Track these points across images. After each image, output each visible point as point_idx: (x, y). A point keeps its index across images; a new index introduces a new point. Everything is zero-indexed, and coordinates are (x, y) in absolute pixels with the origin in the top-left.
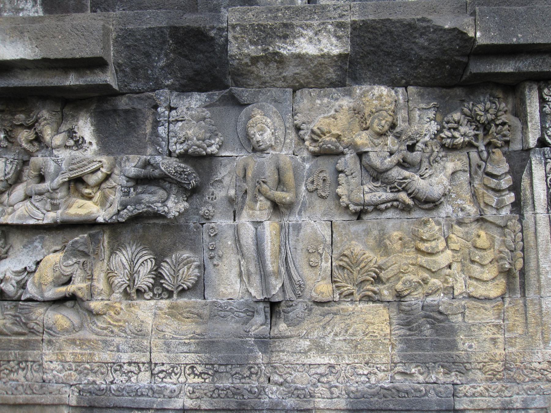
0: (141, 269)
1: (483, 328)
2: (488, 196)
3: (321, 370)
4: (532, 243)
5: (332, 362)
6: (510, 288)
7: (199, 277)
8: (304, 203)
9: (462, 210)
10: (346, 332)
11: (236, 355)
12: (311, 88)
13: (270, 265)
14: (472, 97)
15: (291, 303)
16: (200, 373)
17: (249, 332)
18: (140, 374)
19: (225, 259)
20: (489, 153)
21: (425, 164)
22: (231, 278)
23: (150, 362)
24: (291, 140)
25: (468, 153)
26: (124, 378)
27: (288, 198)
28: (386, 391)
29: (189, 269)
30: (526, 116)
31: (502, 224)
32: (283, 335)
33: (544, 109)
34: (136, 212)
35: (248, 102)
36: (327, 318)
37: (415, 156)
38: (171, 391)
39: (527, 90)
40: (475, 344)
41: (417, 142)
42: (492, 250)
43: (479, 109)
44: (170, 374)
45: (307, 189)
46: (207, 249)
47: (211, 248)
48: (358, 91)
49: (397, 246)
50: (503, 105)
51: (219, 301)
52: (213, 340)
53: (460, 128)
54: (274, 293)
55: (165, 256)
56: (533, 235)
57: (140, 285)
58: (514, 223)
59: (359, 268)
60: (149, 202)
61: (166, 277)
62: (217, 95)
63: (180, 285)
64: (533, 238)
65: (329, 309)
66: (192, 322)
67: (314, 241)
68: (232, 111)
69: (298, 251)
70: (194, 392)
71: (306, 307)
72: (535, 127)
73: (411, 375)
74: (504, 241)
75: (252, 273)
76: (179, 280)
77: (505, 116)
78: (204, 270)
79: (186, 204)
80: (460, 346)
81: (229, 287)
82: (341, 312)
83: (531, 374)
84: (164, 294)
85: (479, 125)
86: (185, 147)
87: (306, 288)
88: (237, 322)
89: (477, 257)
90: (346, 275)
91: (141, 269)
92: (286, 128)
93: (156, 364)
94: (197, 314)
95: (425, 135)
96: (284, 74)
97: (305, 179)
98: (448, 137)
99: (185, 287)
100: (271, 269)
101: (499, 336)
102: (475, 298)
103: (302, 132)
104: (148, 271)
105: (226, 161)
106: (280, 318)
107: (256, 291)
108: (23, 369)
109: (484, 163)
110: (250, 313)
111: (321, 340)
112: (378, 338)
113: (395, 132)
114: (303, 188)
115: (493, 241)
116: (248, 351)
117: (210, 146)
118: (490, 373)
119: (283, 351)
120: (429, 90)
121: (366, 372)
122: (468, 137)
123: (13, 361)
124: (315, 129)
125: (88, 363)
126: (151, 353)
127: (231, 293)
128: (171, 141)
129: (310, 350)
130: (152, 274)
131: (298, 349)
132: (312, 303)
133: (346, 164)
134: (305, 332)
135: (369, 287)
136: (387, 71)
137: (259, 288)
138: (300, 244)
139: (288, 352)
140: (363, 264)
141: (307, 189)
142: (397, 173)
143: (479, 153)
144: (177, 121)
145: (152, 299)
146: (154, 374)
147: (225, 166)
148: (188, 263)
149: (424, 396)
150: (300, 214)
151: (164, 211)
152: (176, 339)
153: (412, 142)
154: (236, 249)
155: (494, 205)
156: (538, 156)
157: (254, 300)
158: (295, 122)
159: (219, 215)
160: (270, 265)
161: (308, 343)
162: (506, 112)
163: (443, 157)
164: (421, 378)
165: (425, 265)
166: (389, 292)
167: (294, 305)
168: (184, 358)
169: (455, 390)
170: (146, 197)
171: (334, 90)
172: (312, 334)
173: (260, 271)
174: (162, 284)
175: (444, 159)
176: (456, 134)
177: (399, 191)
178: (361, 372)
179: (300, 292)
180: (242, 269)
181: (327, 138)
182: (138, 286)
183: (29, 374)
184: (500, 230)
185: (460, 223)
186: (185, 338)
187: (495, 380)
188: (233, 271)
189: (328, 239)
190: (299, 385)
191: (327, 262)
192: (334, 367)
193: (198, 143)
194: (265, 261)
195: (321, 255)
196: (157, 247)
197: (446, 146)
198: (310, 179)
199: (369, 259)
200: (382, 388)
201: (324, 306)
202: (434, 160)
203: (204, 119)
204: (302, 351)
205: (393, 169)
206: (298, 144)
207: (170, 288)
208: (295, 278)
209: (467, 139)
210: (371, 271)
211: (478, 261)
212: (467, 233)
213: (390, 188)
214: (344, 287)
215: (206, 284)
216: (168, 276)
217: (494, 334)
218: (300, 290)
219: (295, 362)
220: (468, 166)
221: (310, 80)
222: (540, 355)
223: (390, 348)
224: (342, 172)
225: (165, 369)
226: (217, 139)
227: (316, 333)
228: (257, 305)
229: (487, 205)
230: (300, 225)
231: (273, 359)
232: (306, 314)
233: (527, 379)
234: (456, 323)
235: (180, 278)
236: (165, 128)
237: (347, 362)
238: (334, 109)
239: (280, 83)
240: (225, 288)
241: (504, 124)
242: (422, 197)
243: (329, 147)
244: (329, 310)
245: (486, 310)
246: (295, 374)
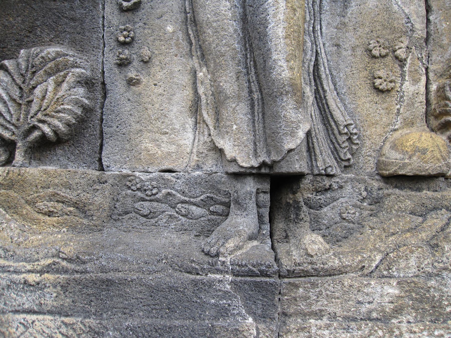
7: (87, 110)
11: (177, 323)
13: (282, 63)
15: (327, 182)
17: (217, 255)
19: (158, 68)
22: (172, 115)
29: (59, 84)
32: (319, 266)
46: (113, 44)
47: (122, 39)
51: (137, 174)
52: (111, 275)
54: (292, 146)
63: (34, 128)
65: (438, 195)
66: (61, 224)
67: (384, 27)
69: (344, 53)
71: (364, 194)
75: (227, 98)
76: (32, 111)
78: (105, 97)
81: (165, 138)
87: (363, 145)
88: (183, 230)
94: (75, 205)
99: (46, 129)
100: (286, 74)
106: (298, 220)
107: (238, 144)
110: (219, 208)
111: (432, 283)
116: (213, 313)
119: (319, 315)
127: (169, 154)
129: (398, 311)
131: (364, 309)
132: (382, 184)
134: (378, 258)
137: (247, 137)
138: (350, 35)
139: (333, 317)
154: (185, 44)
157: (233, 169)
160: (282, 63)
167: (335, 186)
168: (22, 329)
172: (403, 264)
179: (349, 156)
180: (201, 91)
186: (29, 267)
188: (177, 97)
191: (416, 81)
195: (402, 62)
201: (419, 190)
204: (374, 315)
215: (105, 129)
218: (350, 150)
227: (413, 262)
228: (239, 186)
232: (366, 213)
235: (34, 108)
240: (155, 140)
244: (436, 199)
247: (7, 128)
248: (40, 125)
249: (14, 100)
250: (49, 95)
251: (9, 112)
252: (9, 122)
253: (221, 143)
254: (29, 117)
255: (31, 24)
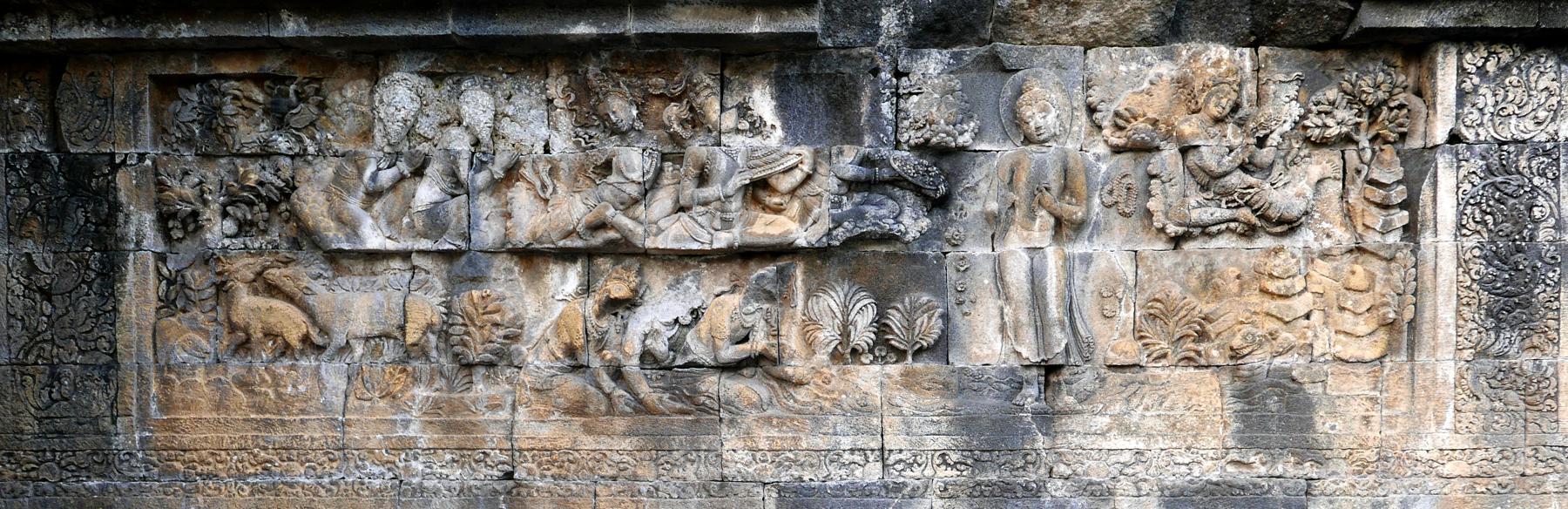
0: (859, 318)
1: (1352, 401)
2: (1371, 214)
3: (1126, 457)
4: (1429, 284)
5: (1142, 446)
6: (1391, 349)
8: (1097, 224)
9: (1328, 236)
10: (1161, 404)
12: (1112, 46)
14: (1355, 65)
16: (955, 463)
18: (868, 465)
20: (1374, 152)
21: (1278, 168)
23: (882, 449)
24: (1080, 127)
25: (1343, 152)
26: (843, 472)
27: (1080, 214)
28: (1215, 487)
29: (930, 318)
30: (1434, 95)
31: (1387, 256)
33: (1463, 86)
34: (857, 231)
35: (1018, 67)
36: (1132, 388)
37: (1265, 155)
38: (913, 490)
39: (1440, 55)
40: (1339, 425)
41: (1272, 132)
42: (1371, 293)
43: (1366, 84)
44: (911, 465)
45: (1103, 202)
48: (1184, 53)
49: (1233, 286)
50: (1402, 78)
53: (1336, 112)
55: (890, 301)
56: (1432, 272)
58: (1404, 255)
59: (1177, 318)
60: (875, 217)
61: (896, 331)
62: (971, 51)
64: (1431, 277)
66: (938, 394)
68: (991, 78)
70: (946, 489)
72: (1447, 112)
73: (1249, 465)
74: (1388, 280)
77: (1403, 95)
79: (928, 220)
80: (1319, 427)
82: (1150, 380)
83: (1416, 466)
85: (1364, 109)
86: (927, 136)
89: (1350, 302)
90: (1158, 328)
91: (859, 318)
92: (1074, 109)
93: (891, 451)
95: (1285, 122)
96: (1075, 23)
97: (1100, 187)
98: (1317, 126)
99: (925, 344)
101: (1373, 413)
102: (1342, 360)
103: (1098, 115)
104: (870, 321)
105: (982, 158)
108: (693, 462)
109: (1366, 167)
112: (1206, 413)
113: (1236, 117)
114: (1097, 201)
115: (1373, 281)
117: (961, 134)
118: (1359, 463)
119: (1071, 432)
120: (1290, 52)
121: (1187, 460)
122: (1346, 125)
123: (678, 450)
124: (1121, 109)
125: (790, 450)
126: (882, 435)
128: (900, 125)
129: (1109, 430)
131: (1093, 429)
133: (1163, 165)
134: (1102, 406)
135: (1192, 345)
136: (1230, 21)
137: (1034, 346)
139: (1079, 433)
140: (1183, 313)
141: (1103, 202)
142: (1236, 179)
143: (1360, 151)
144: (911, 94)
145: (872, 362)
146: (888, 465)
147: (980, 165)
148: (930, 309)
149: (1267, 493)
150: (1090, 239)
151: (900, 231)
152: (918, 415)
153: (1264, 132)
155: (1378, 228)
156: (1448, 157)
157: (1027, 363)
158: (1090, 99)
159: (971, 240)
161: (1107, 420)
162: (1405, 88)
163: (1305, 156)
164: (1263, 470)
165: (1274, 313)
166: (1220, 353)
169: (1309, 486)
170: (871, 210)
171: (1146, 50)
172: (1112, 408)
173: (1036, 322)
174: (888, 340)
175: (1307, 159)
176: (1330, 121)
177: (1239, 206)
178: (1180, 460)
180: (1006, 319)
181: (1140, 124)
183: (702, 468)
184: (1384, 264)
185: (1325, 255)
187: (1365, 473)
189: (1131, 277)
190: (1095, 479)
192: (1142, 454)
193: (947, 128)
194: (1046, 306)
196: (879, 288)
197: (1313, 139)
198: (1108, 187)
199: (1192, 305)
200: (1209, 482)
202: (1293, 161)
203: (953, 91)
205: (1234, 173)
206: (1090, 134)
207: (902, 347)
208: (1082, 332)
209: (1344, 129)
210: (1195, 322)
211: (1351, 307)
212: (1336, 269)
213: (1227, 203)
214: (1154, 344)
216: (899, 328)
217: (1368, 410)
219: (1090, 447)
220: (1341, 171)
221: (1113, 34)
222: (1429, 439)
223: (1221, 429)
224: (1154, 177)
225: (904, 458)
226: (972, 124)
227: (1118, 407)
229: (1367, 227)
230: (1091, 254)
231: (1059, 442)
233: (1409, 473)
234: (1314, 394)
235: (917, 331)
236: (892, 104)
237: (1163, 447)
238: (1147, 80)
239: (1065, 38)
241: (1401, 107)
242: (1274, 214)
243: (1143, 138)
245: (1357, 376)
246: (1088, 463)
250: (925, 324)
253: (1019, 349)
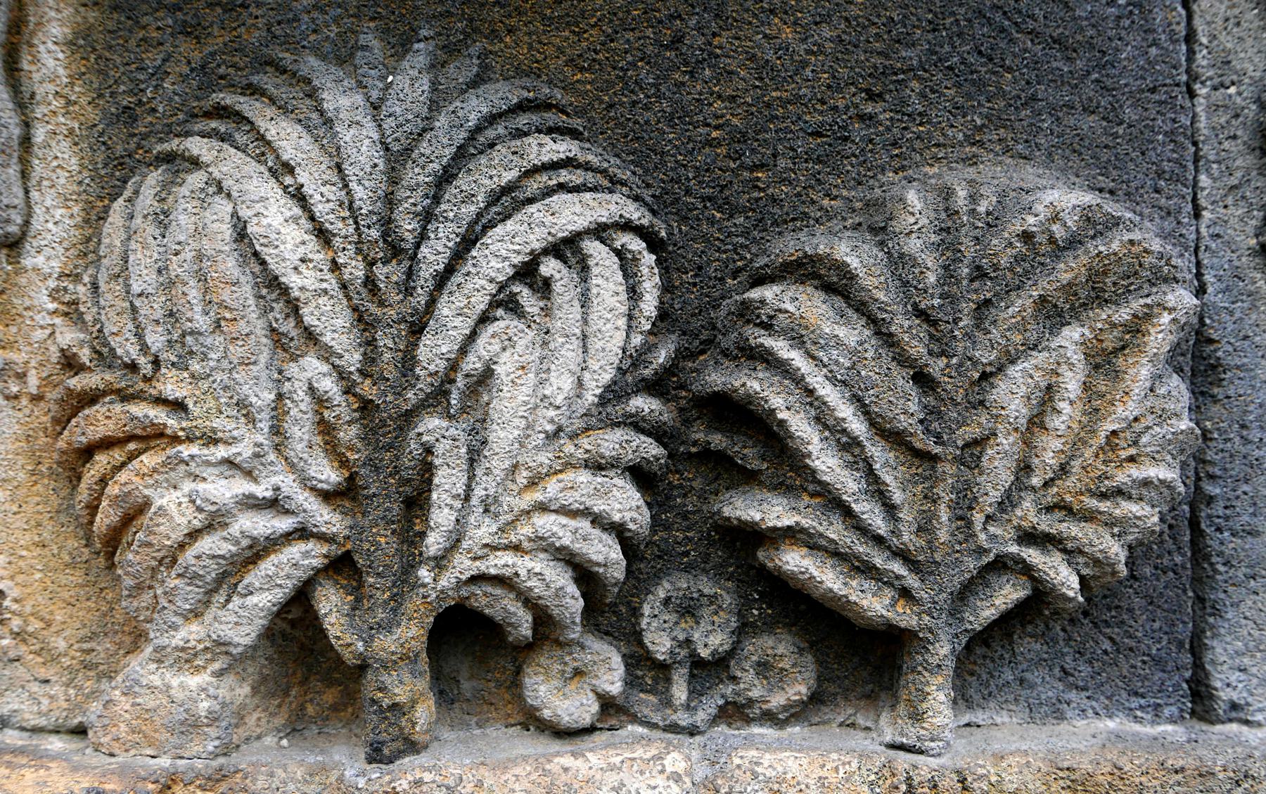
57: (500, 563)
63: (1001, 565)
84: (763, 668)
130: (637, 424)
182: (463, 566)
216: (848, 446)
247: (865, 569)
248: (1032, 555)
249: (895, 438)
250: (1066, 415)
251: (878, 492)
252: (879, 540)
254: (978, 518)
255: (878, 61)
